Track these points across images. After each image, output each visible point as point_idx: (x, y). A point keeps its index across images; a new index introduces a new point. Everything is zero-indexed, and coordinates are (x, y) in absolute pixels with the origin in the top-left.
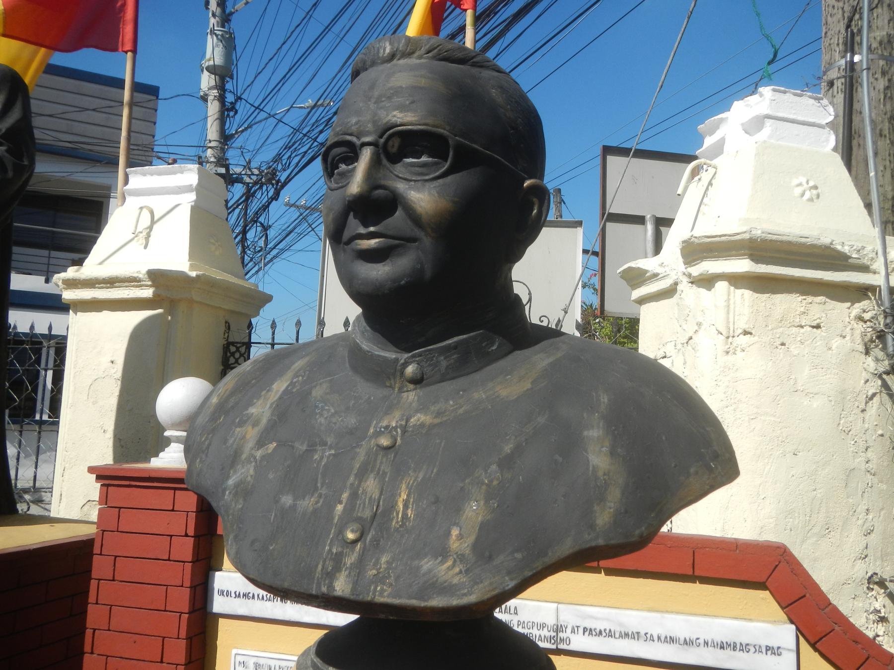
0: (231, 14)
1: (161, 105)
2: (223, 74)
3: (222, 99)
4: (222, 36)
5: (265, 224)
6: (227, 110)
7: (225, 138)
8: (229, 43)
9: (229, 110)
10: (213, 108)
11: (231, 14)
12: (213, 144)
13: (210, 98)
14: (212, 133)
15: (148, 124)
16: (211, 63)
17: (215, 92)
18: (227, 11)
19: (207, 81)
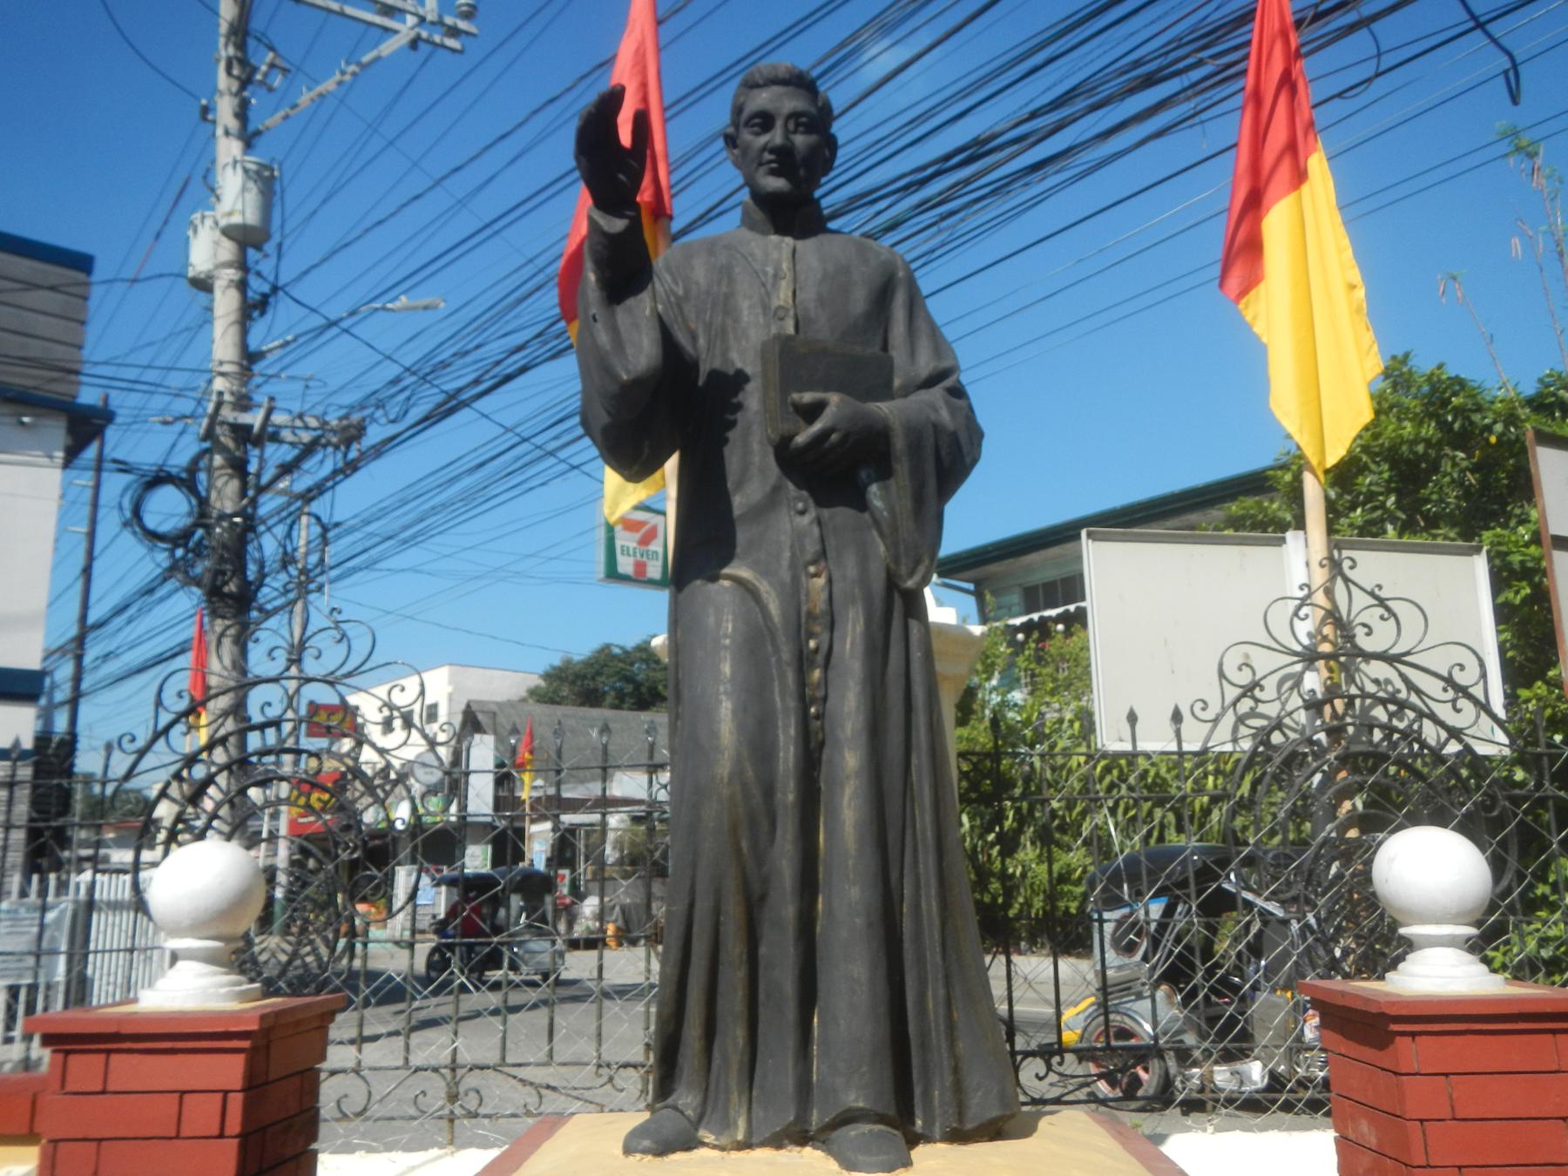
0: (258, 133)
1: (97, 292)
2: (246, 239)
3: (242, 286)
4: (258, 173)
5: (325, 520)
6: (252, 309)
7: (249, 357)
8: (267, 182)
9: (254, 307)
10: (225, 303)
11: (258, 133)
12: (226, 368)
13: (219, 285)
14: (223, 345)
15: (72, 324)
16: (237, 219)
17: (232, 274)
18: (251, 128)
19: (206, 250)
